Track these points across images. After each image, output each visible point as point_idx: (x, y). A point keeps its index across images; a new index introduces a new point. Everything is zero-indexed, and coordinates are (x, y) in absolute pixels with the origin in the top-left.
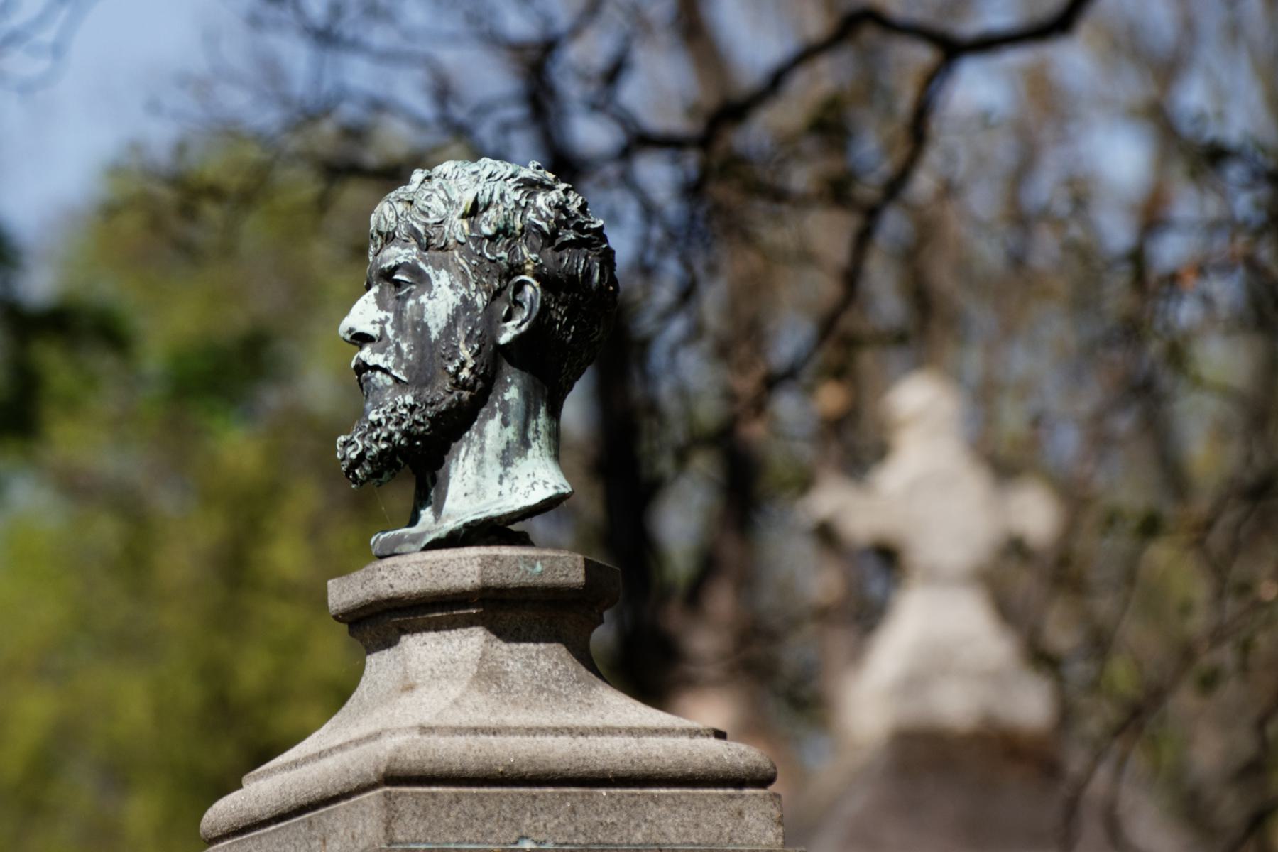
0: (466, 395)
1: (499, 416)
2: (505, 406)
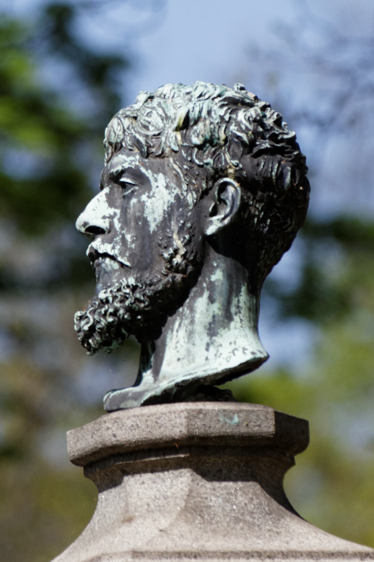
0: (179, 277)
1: (206, 294)
2: (212, 286)
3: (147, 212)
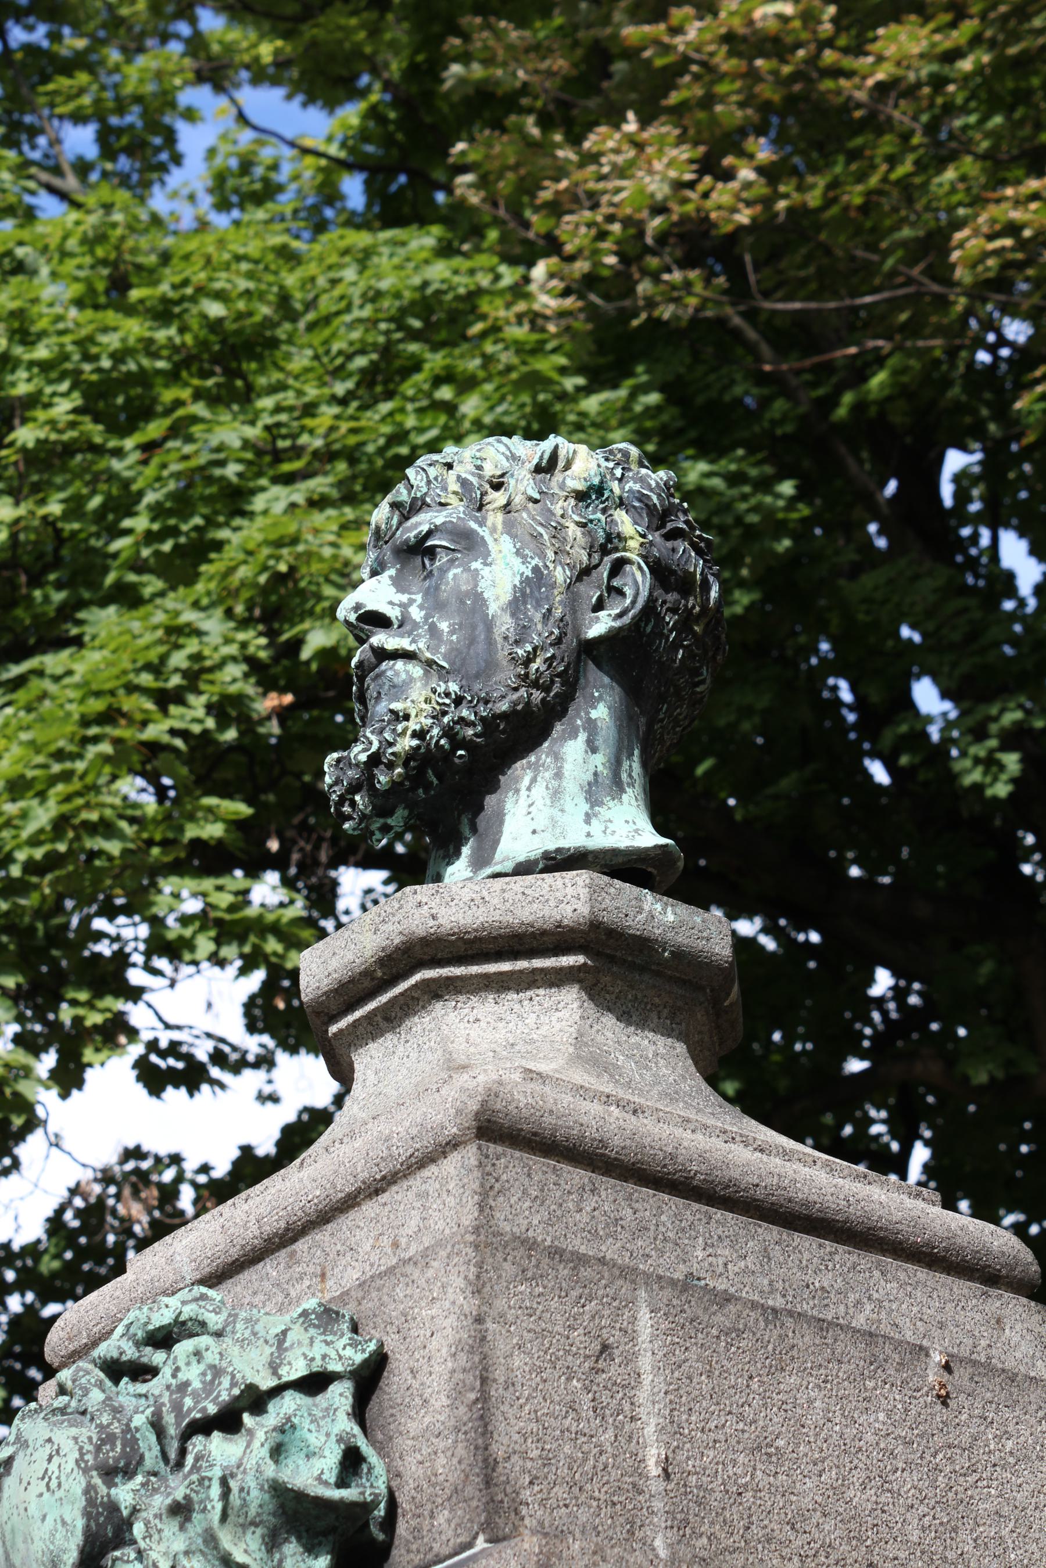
0: (537, 695)
1: (582, 737)
2: (591, 726)
3: (482, 585)
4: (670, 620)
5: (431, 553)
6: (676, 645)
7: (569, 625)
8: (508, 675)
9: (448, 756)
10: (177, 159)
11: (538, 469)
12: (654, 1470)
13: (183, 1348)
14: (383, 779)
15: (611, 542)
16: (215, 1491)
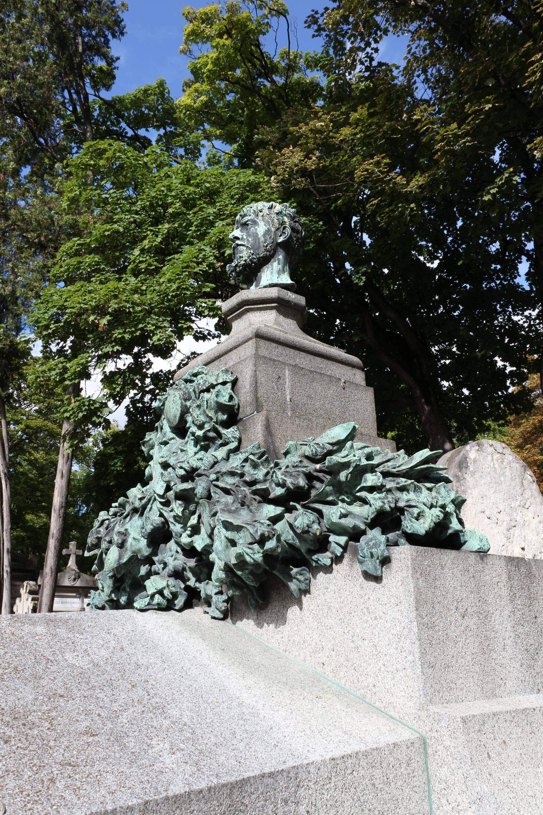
0: (268, 253)
2: (279, 260)
4: (295, 239)
5: (248, 225)
6: (296, 244)
7: (275, 239)
8: (263, 249)
9: (251, 265)
10: (201, 155)
11: (269, 208)
12: (288, 400)
13: (199, 377)
14: (238, 269)
15: (283, 223)
16: (205, 403)
